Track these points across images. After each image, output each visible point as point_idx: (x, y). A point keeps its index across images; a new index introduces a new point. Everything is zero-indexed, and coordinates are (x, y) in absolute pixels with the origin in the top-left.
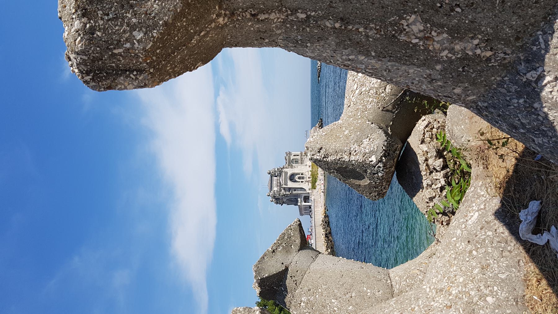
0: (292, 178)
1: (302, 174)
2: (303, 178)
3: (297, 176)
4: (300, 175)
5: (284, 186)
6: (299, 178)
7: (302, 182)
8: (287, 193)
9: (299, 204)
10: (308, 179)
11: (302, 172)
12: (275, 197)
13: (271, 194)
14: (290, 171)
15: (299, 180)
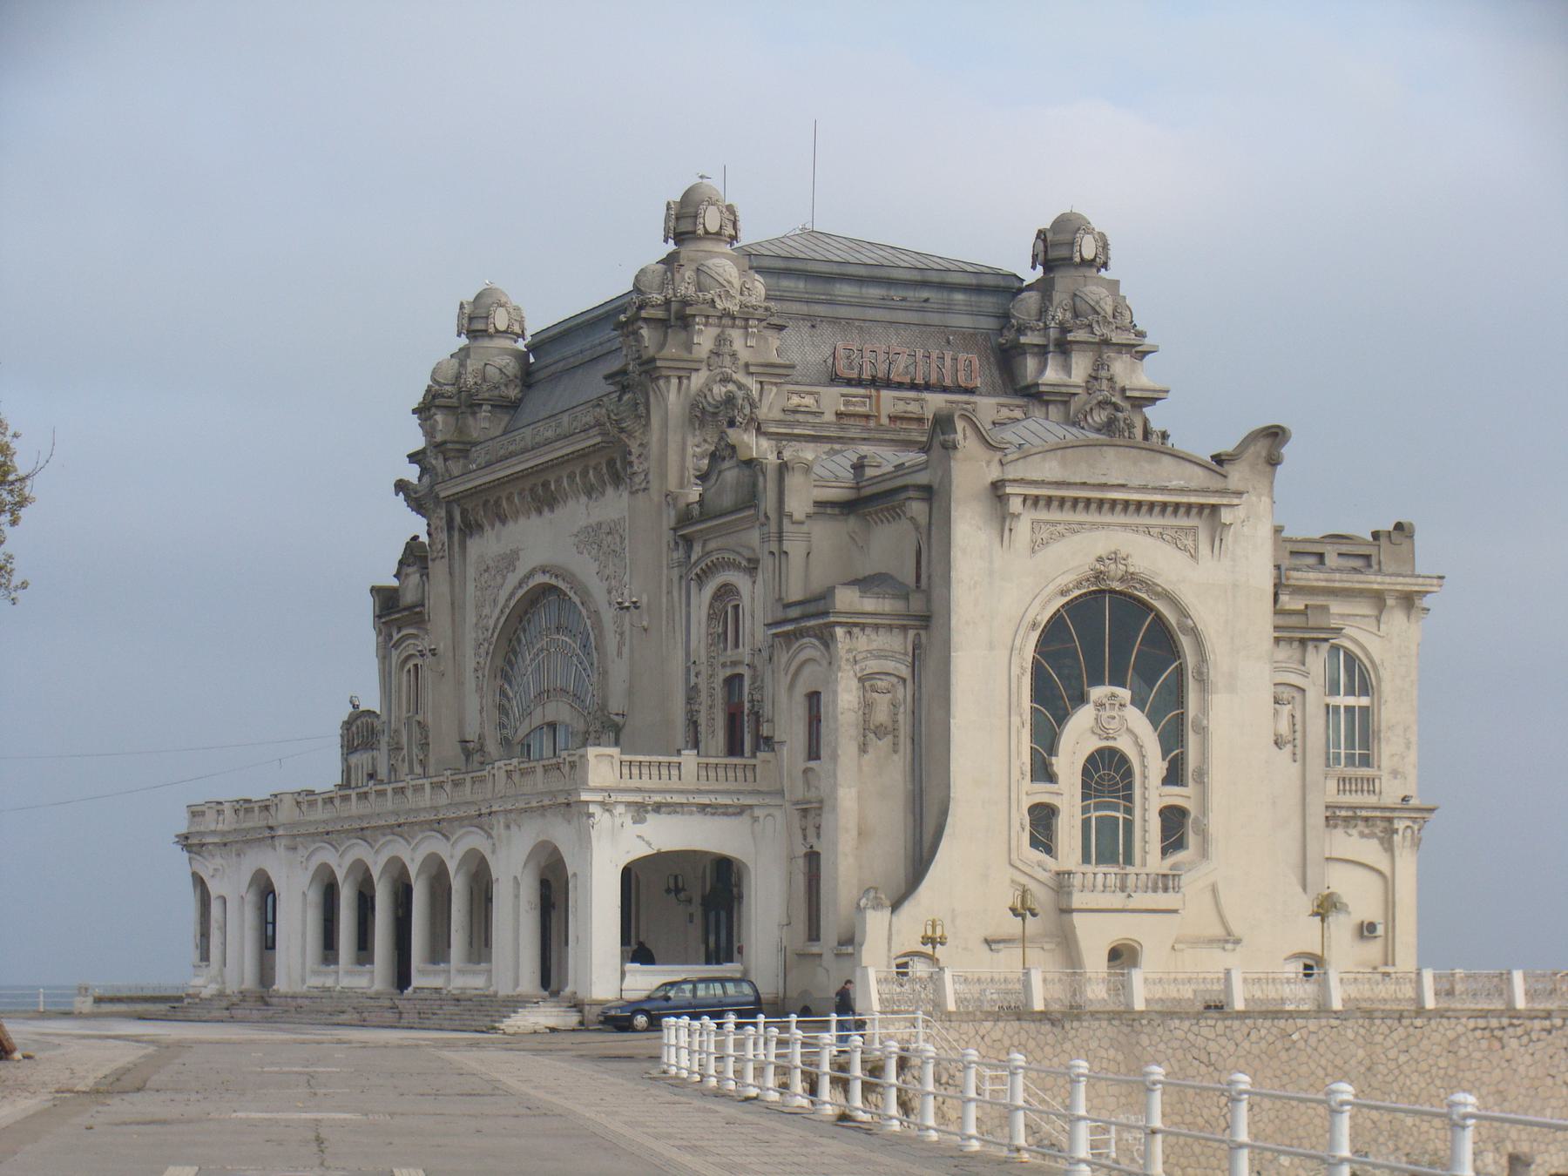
0: (1112, 640)
1: (1175, 824)
2: (1109, 845)
3: (1136, 735)
4: (1152, 795)
5: (971, 470)
6: (1108, 774)
7: (1043, 820)
8: (813, 553)
9: (602, 766)
10: (1095, 937)
11: (1216, 823)
12: (678, 318)
13: (725, 267)
14: (1220, 589)
15: (1079, 737)
